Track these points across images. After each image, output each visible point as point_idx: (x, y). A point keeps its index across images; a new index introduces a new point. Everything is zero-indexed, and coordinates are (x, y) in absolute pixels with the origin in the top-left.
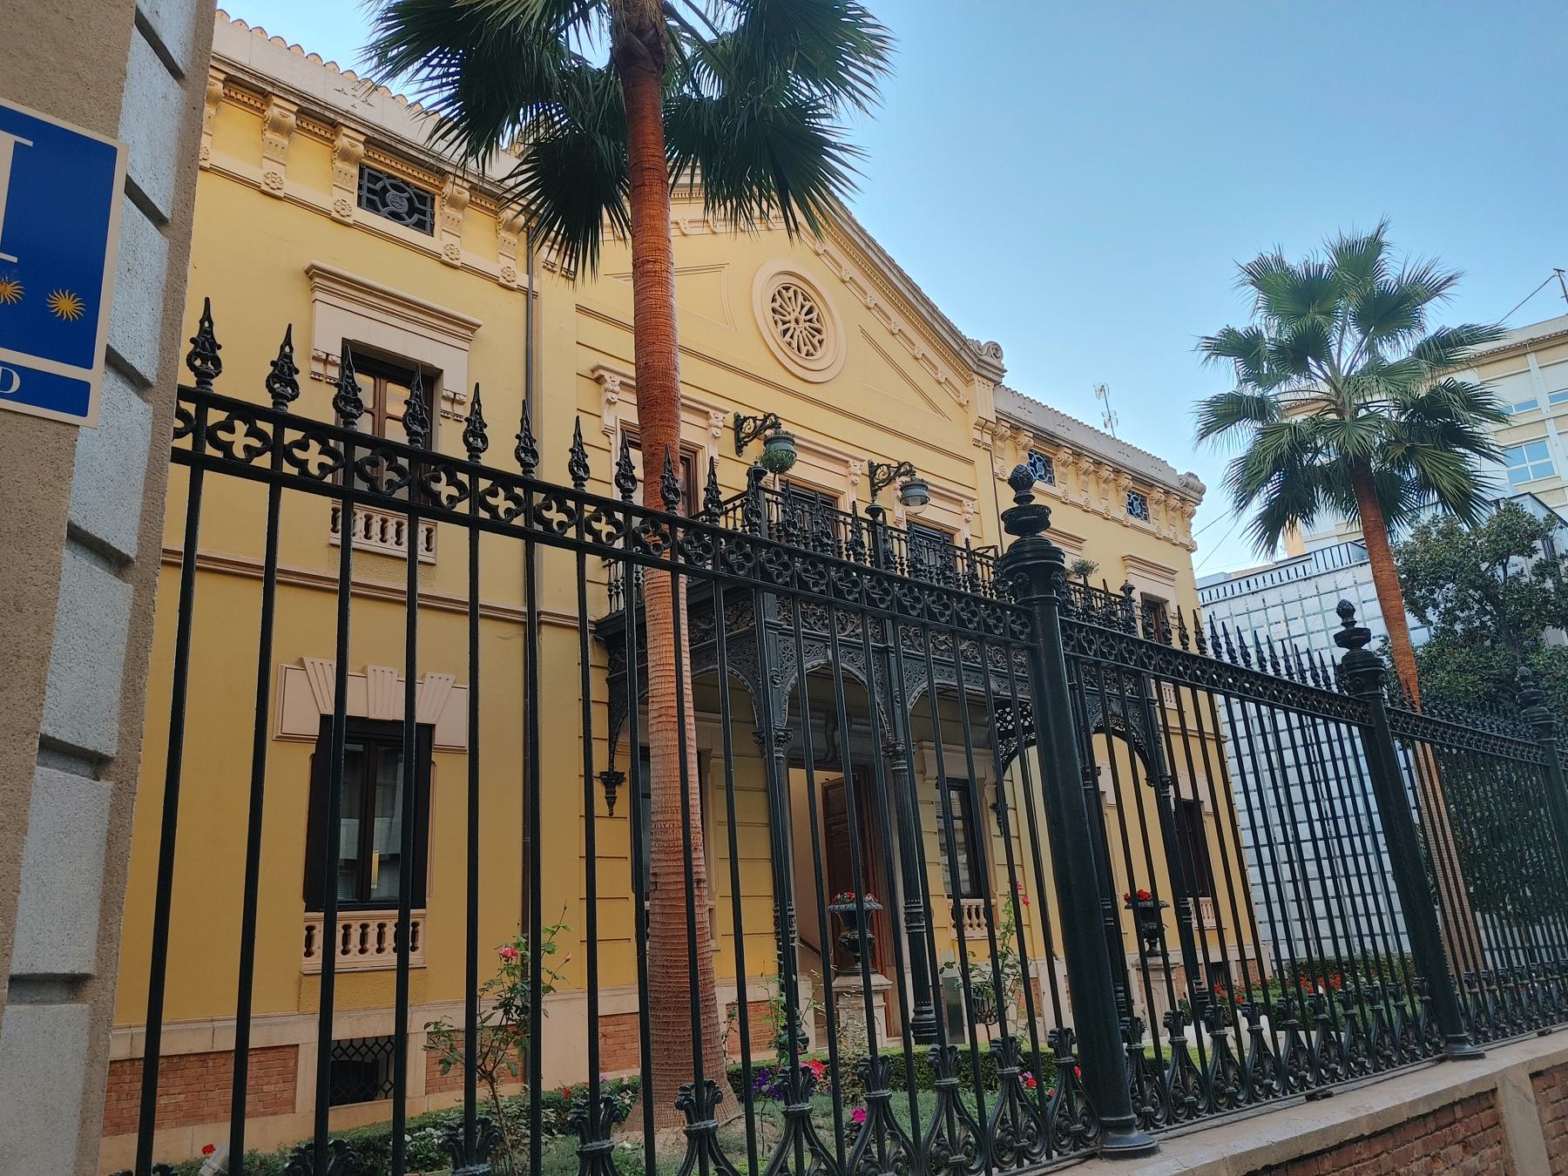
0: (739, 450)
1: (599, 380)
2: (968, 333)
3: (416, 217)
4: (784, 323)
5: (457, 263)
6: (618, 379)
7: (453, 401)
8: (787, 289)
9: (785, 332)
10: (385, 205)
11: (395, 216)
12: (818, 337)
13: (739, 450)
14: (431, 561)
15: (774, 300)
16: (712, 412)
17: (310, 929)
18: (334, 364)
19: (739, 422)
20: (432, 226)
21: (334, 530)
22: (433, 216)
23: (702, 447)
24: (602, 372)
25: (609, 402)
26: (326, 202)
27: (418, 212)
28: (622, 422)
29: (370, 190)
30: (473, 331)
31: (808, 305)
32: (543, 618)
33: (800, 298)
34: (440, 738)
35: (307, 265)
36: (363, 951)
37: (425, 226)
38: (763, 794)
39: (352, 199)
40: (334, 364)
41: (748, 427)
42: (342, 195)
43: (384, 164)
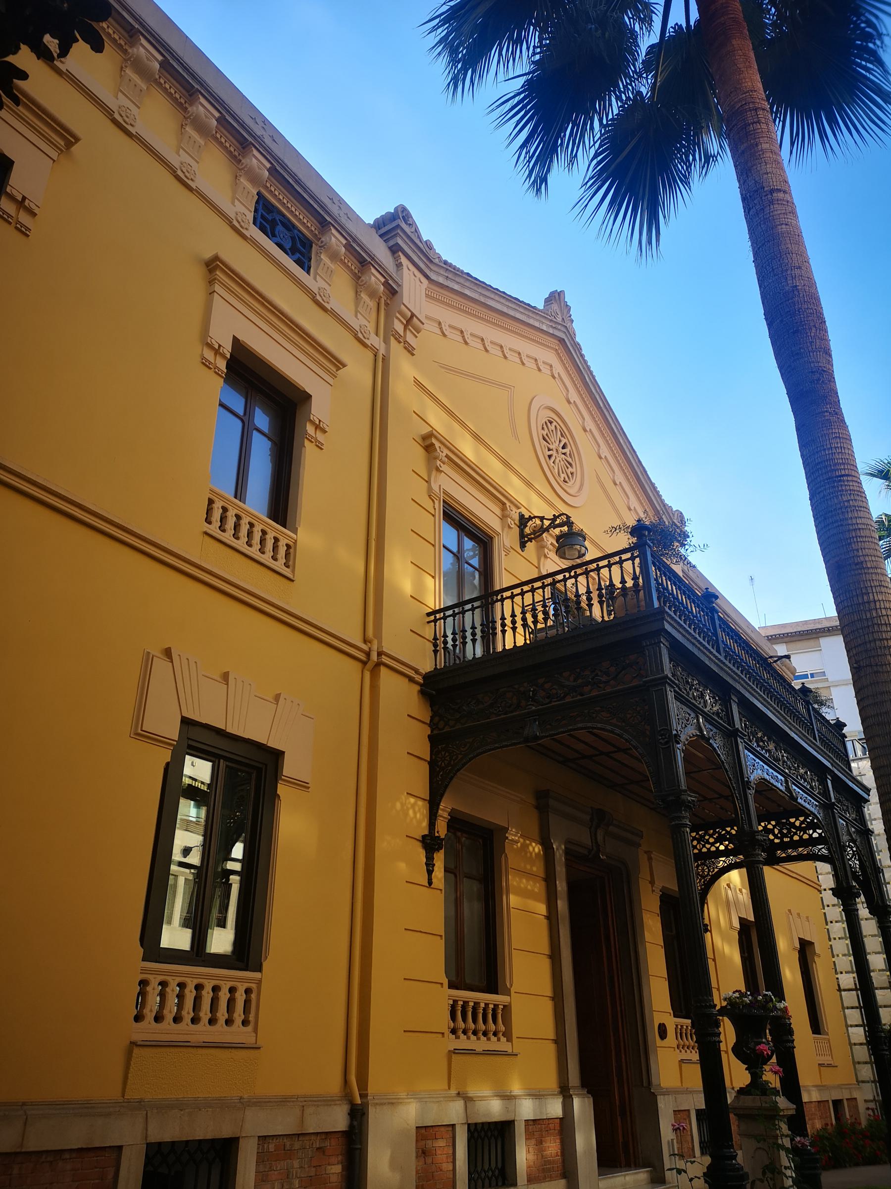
0: (523, 545)
1: (429, 448)
2: (668, 501)
3: (298, 255)
4: (549, 450)
5: (328, 306)
6: (446, 451)
7: (317, 427)
8: (551, 423)
9: (550, 456)
10: (274, 235)
11: (279, 245)
12: (570, 469)
13: (523, 545)
14: (291, 576)
15: (543, 428)
16: (508, 504)
17: (143, 983)
18: (223, 356)
19: (523, 521)
20: (309, 268)
21: (210, 523)
22: (310, 259)
23: (498, 534)
24: (434, 441)
25: (438, 470)
26: (230, 210)
27: (301, 250)
28: (445, 492)
29: (263, 217)
30: (338, 369)
31: (564, 441)
32: (385, 659)
33: (559, 433)
34: (289, 768)
35: (208, 255)
36: (195, 1020)
37: (304, 263)
38: (543, 883)
39: (250, 216)
40: (223, 356)
41: (527, 530)
42: (244, 211)
43: (280, 200)
